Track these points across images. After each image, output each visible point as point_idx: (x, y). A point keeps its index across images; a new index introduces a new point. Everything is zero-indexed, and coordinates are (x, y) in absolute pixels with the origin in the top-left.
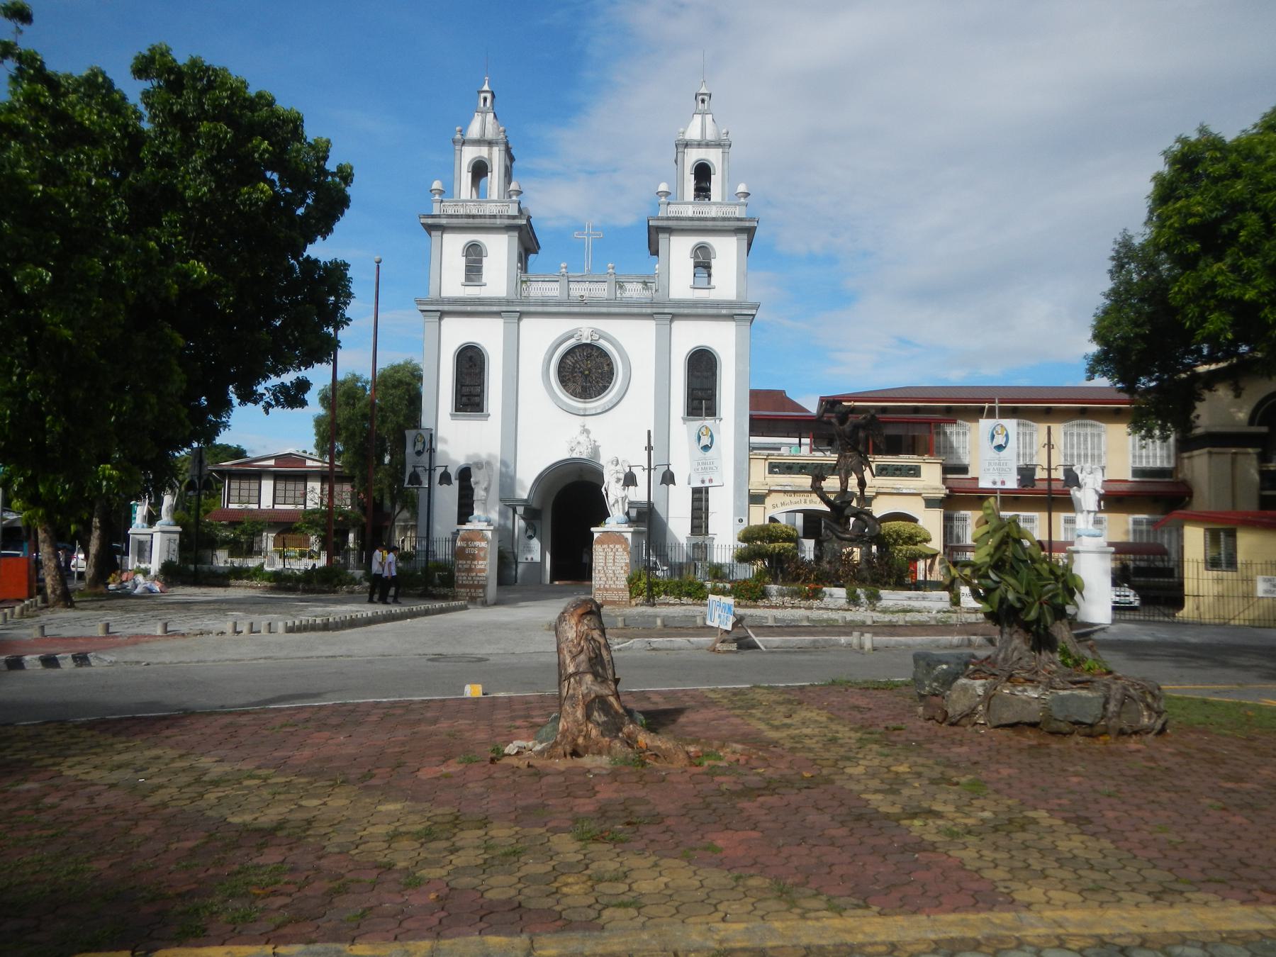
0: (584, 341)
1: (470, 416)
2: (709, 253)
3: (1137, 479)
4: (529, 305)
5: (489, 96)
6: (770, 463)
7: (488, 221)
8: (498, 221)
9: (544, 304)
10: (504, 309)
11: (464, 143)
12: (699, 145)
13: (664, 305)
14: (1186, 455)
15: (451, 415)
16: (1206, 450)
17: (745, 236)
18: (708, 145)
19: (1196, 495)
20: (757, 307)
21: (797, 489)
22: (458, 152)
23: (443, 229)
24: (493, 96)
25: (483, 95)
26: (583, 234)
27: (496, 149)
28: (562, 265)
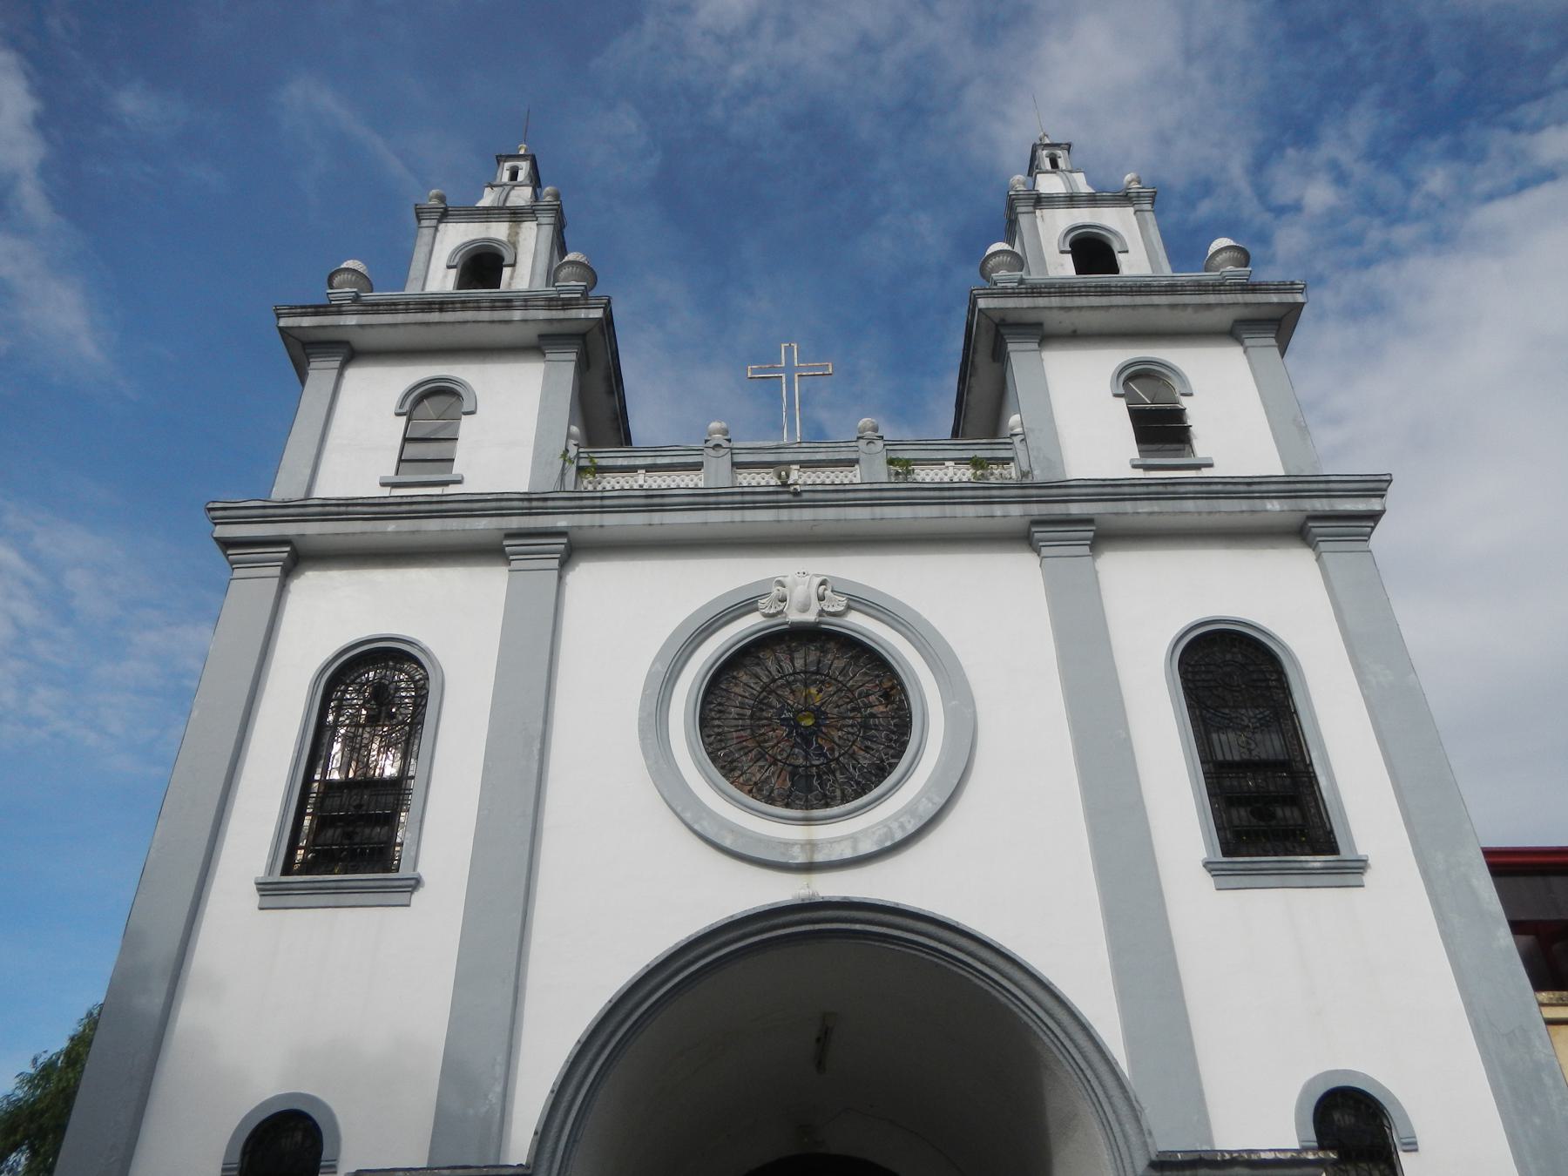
0: (794, 616)
1: (338, 890)
2: (1170, 388)
4: (603, 510)
5: (524, 167)
8: (517, 315)
9: (653, 502)
10: (515, 523)
11: (445, 215)
12: (1072, 200)
13: (1064, 490)
15: (265, 888)
18: (1093, 200)
20: (1377, 486)
22: (426, 234)
23: (351, 353)
25: (507, 165)
26: (773, 369)
27: (529, 231)
28: (714, 425)
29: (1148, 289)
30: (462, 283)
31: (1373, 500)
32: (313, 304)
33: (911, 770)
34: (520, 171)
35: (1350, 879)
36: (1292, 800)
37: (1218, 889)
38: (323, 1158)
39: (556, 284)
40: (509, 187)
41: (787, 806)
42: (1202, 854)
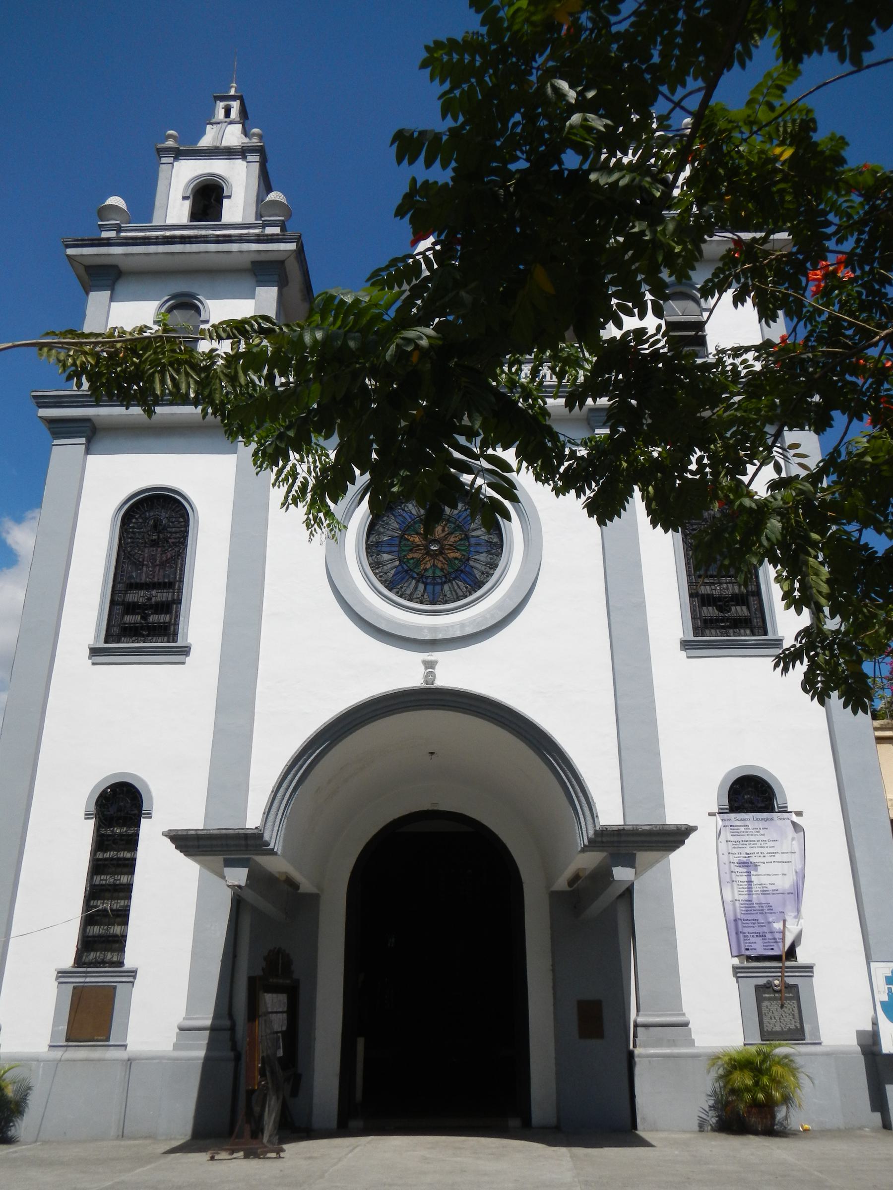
5: (235, 105)
7: (212, 247)
8: (235, 247)
11: (178, 154)
24: (244, 113)
30: (195, 215)
32: (90, 238)
33: (501, 579)
34: (232, 109)
37: (688, 657)
38: (143, 809)
39: (263, 219)
40: (226, 124)
41: (422, 603)
42: (679, 635)
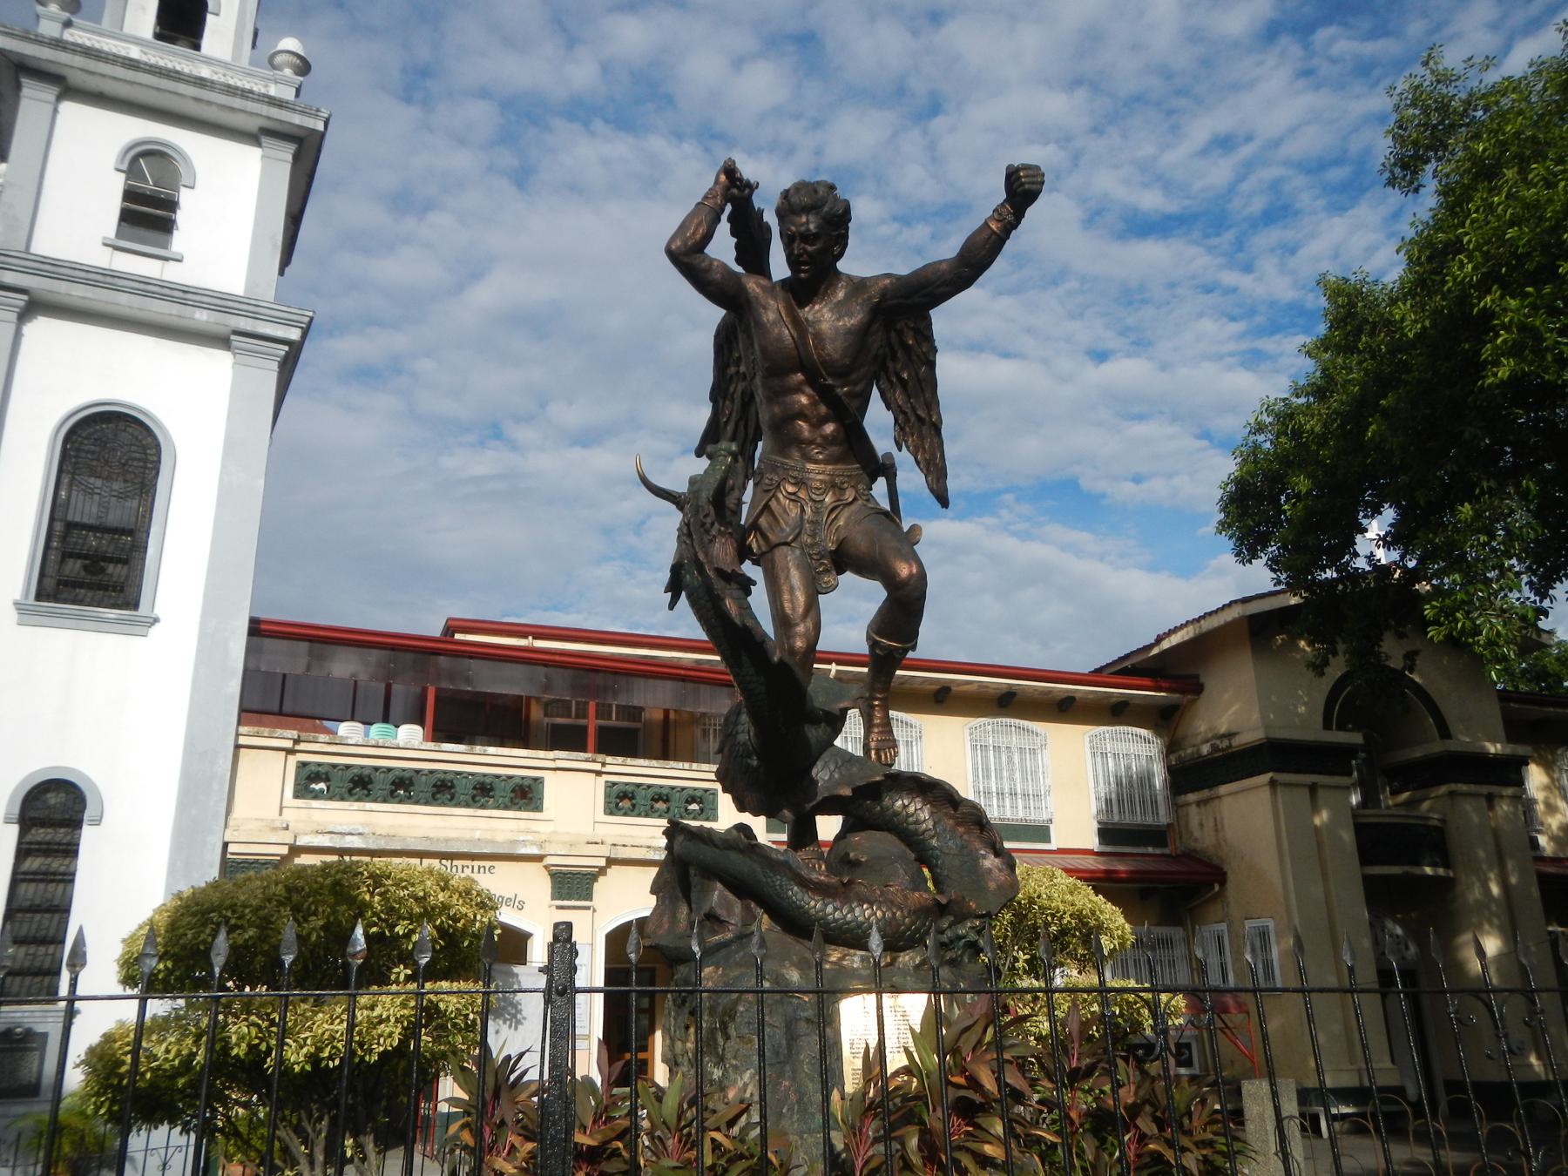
3: (1108, 849)
6: (303, 765)
14: (1192, 797)
16: (1265, 778)
17: (286, 153)
19: (1231, 877)
21: (381, 844)
29: (177, 76)
31: (293, 329)
35: (137, 629)
36: (125, 562)
42: (18, 595)
